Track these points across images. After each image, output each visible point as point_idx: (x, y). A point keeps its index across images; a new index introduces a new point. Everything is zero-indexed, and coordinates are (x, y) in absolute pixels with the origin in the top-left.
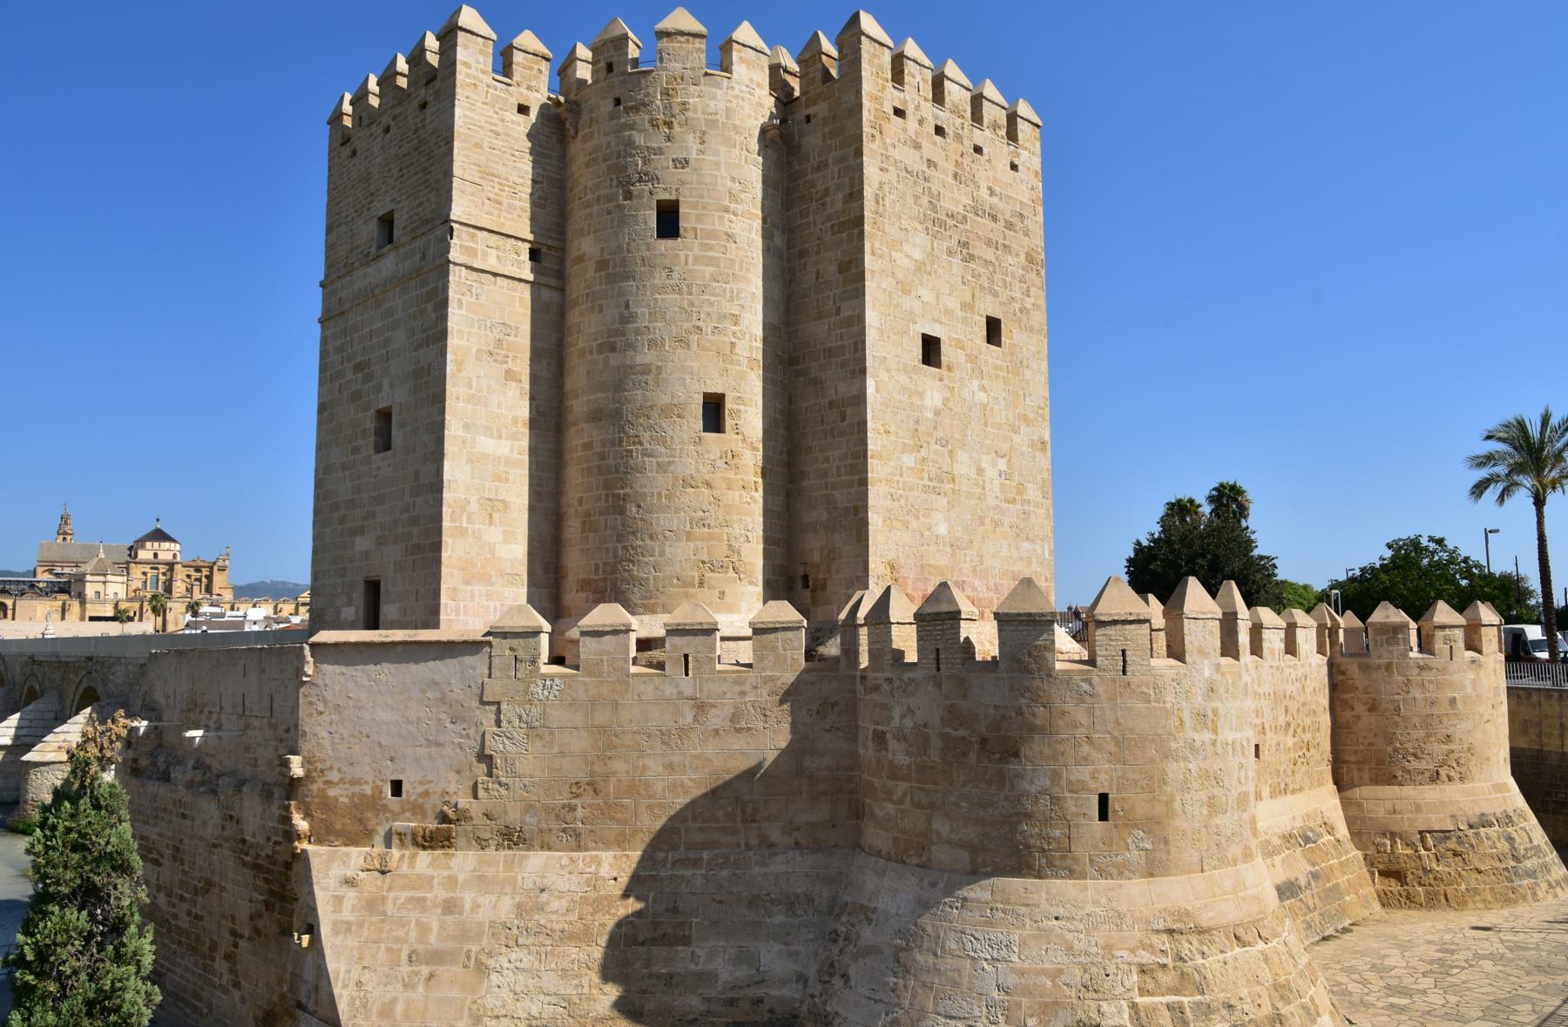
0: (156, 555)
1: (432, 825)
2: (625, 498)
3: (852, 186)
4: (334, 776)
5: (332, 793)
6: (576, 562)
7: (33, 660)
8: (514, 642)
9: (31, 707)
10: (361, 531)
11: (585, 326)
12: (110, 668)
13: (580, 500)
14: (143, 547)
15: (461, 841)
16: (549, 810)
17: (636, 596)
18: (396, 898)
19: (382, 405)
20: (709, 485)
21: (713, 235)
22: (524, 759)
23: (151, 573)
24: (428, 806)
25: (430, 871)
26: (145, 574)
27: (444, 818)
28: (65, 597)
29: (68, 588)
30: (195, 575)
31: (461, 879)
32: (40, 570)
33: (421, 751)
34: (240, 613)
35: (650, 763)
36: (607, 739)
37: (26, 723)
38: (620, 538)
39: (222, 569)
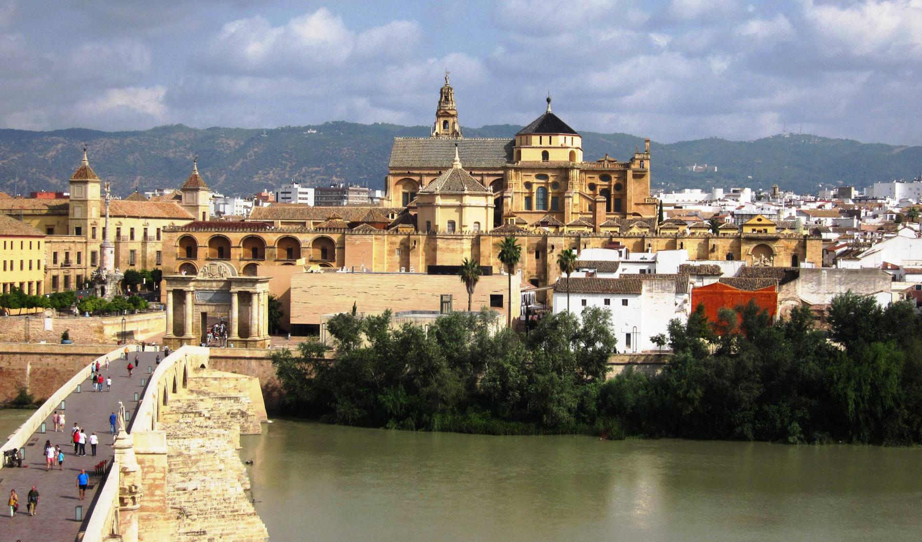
0: (545, 155)
14: (528, 144)
26: (528, 185)
28: (409, 229)
30: (601, 184)
39: (638, 176)
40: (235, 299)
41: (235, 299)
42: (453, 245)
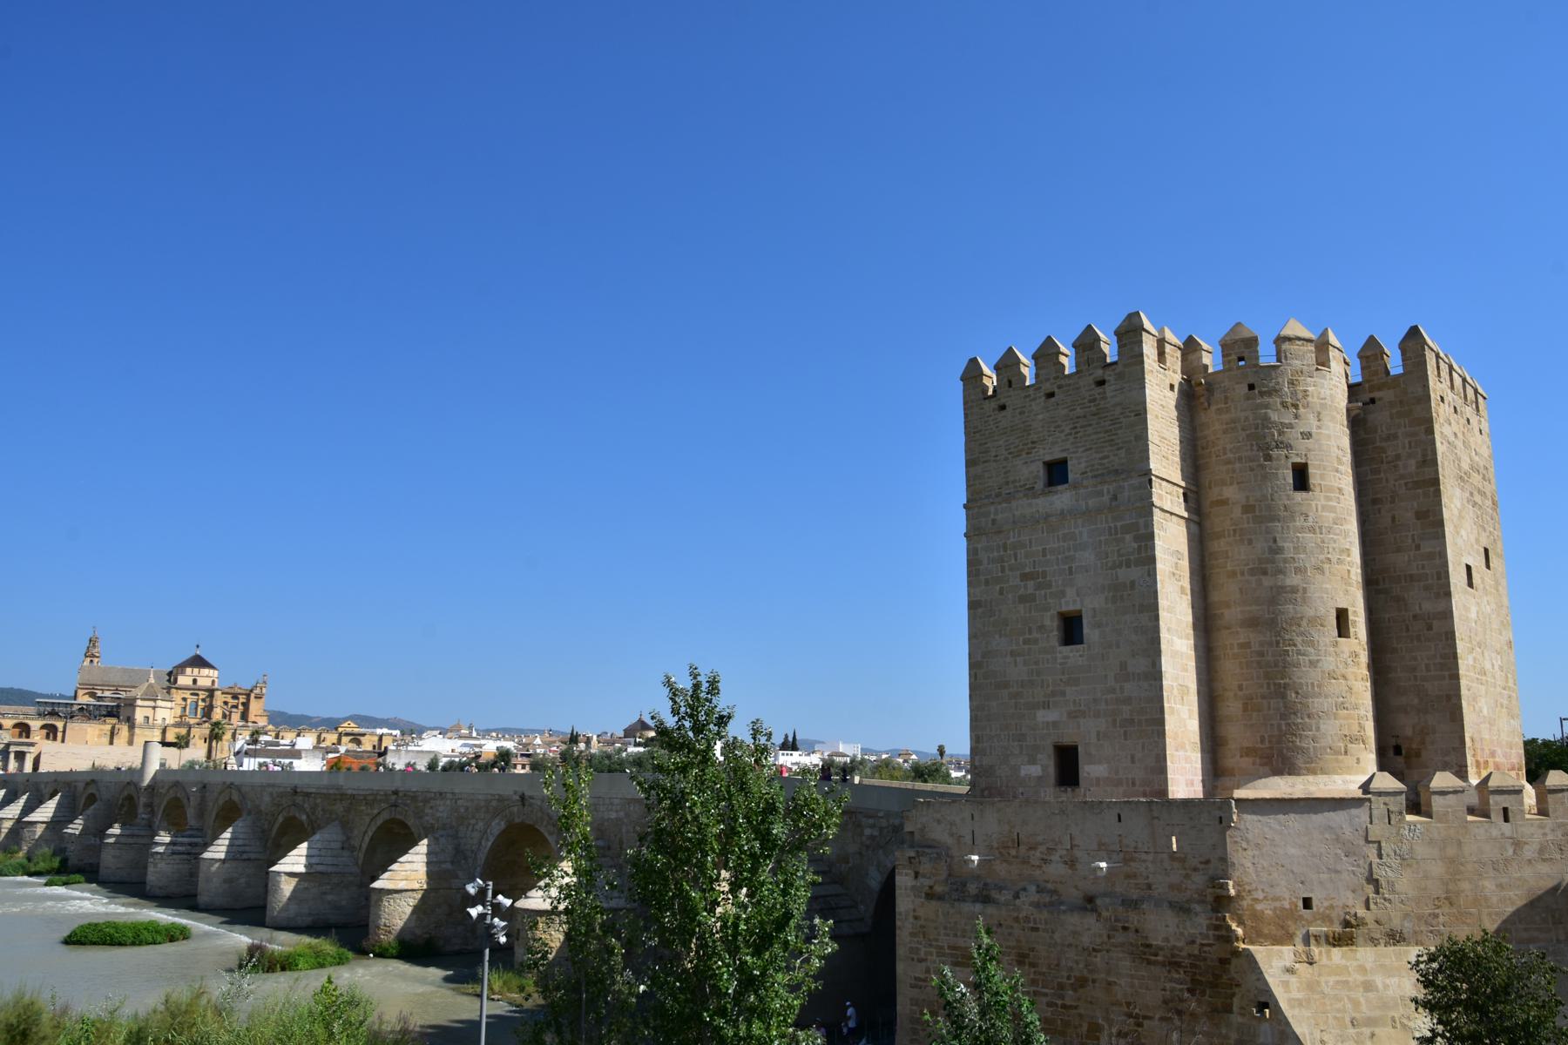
0: (195, 681)
1: (1338, 929)
2: (1286, 686)
3: (1424, 455)
4: (1260, 895)
5: (1259, 907)
6: (1237, 734)
7: (295, 792)
8: (1387, 799)
9: (317, 837)
10: (1046, 706)
11: (1233, 555)
12: (426, 801)
13: (1240, 688)
14: (183, 673)
15: (1360, 940)
16: (1420, 918)
17: (1300, 762)
18: (1328, 982)
19: (1069, 606)
20: (1344, 677)
21: (1330, 489)
22: (1403, 882)
23: (191, 699)
24: (1334, 915)
25: (1344, 962)
26: (185, 699)
27: (1347, 924)
28: (114, 721)
29: (117, 712)
30: (232, 702)
31: (1368, 966)
32: (81, 692)
33: (1324, 876)
34: (286, 741)
35: (1487, 883)
36: (1454, 865)
37: (315, 852)
38: (1283, 716)
39: (258, 697)
40: (12, 756)
41: (12, 756)
42: (147, 732)
